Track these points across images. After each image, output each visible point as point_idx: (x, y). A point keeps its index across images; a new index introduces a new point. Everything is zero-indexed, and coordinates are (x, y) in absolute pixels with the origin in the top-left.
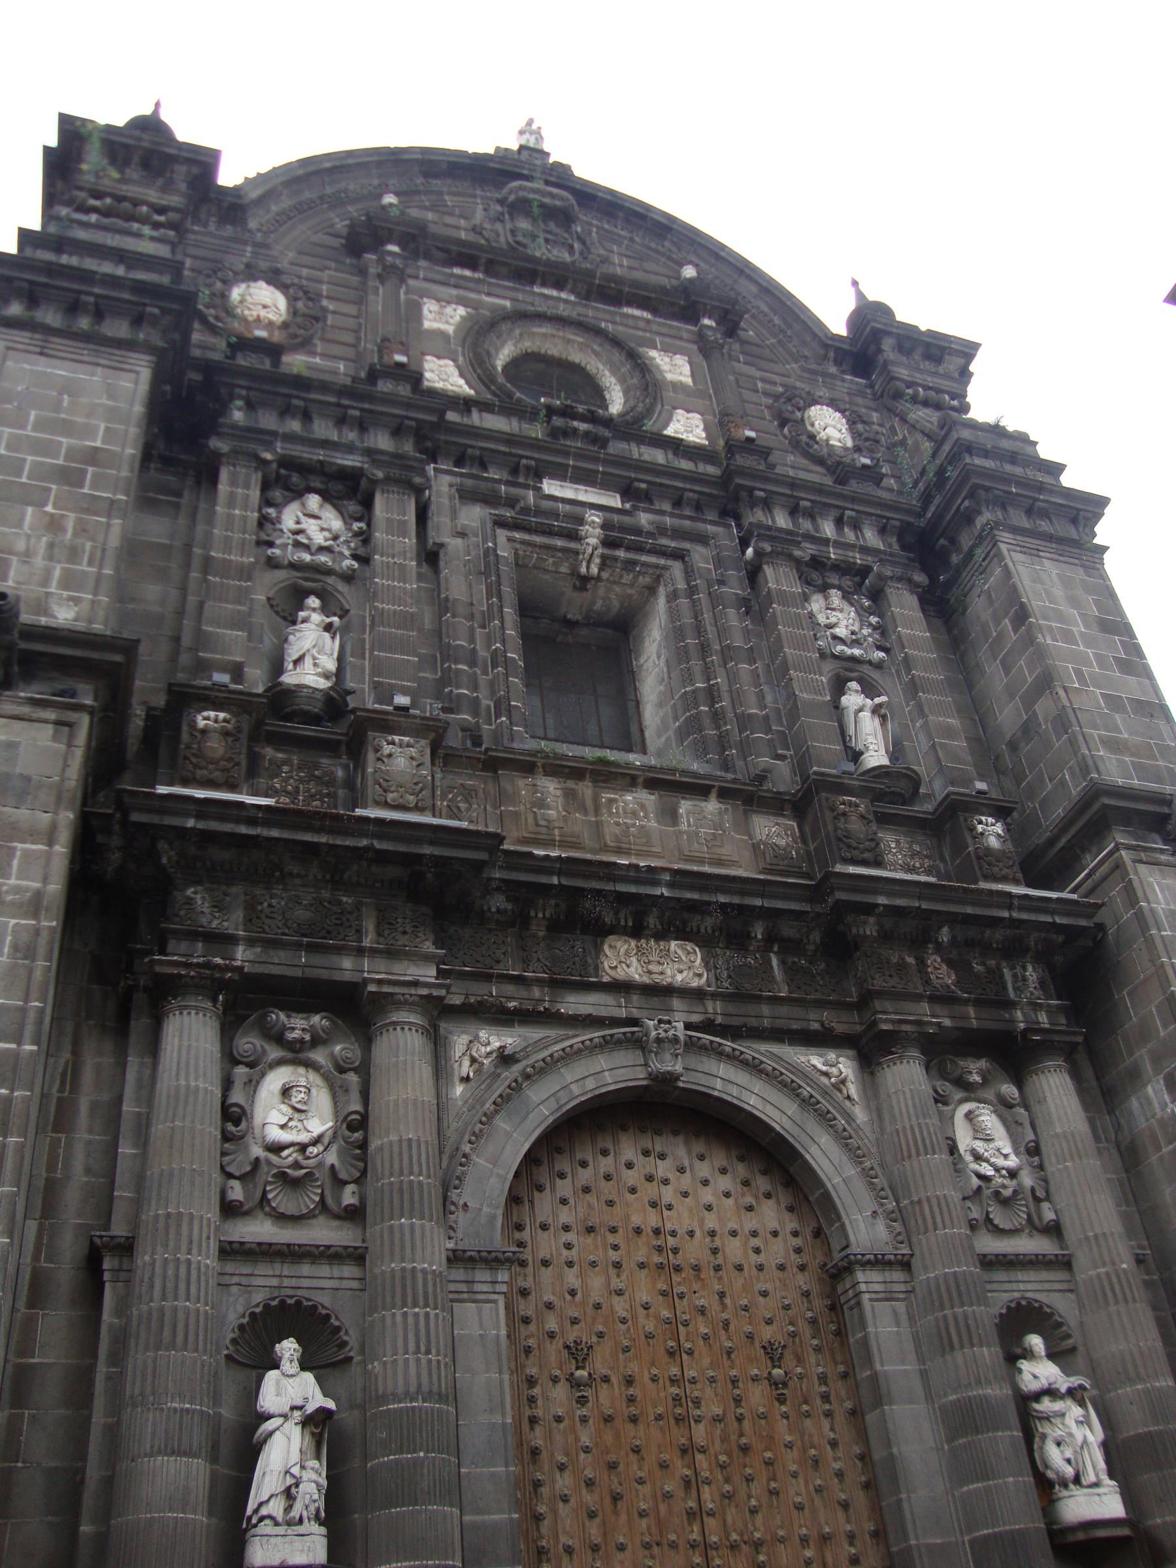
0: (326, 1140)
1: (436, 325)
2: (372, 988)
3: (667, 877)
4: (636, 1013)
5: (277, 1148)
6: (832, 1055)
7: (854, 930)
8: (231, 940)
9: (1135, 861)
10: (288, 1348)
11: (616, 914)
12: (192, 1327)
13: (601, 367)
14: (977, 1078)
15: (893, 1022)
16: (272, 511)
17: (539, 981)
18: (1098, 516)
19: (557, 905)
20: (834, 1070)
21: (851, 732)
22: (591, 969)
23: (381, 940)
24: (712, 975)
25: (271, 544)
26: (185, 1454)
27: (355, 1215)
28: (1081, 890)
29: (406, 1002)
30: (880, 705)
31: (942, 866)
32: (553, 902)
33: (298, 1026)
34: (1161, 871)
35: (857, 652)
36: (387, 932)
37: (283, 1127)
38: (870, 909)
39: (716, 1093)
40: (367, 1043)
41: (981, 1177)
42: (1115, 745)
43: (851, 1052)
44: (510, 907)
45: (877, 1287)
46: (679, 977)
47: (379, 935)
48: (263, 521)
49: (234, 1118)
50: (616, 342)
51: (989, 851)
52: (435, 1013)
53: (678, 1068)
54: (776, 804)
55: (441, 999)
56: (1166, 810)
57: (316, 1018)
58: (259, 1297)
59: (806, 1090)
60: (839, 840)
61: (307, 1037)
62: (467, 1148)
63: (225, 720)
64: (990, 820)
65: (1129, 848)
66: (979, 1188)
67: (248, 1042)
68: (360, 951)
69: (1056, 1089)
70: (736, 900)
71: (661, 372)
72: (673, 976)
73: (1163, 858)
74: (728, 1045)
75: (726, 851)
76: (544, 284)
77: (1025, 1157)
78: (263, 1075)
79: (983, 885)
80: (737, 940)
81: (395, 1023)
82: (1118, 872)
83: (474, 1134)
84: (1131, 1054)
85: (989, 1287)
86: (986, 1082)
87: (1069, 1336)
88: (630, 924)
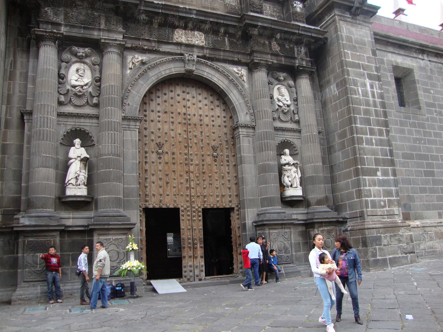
0: (89, 85)
2: (103, 41)
3: (195, 12)
4: (183, 52)
5: (74, 87)
6: (240, 68)
7: (251, 32)
8: (59, 25)
9: (340, 20)
10: (77, 141)
11: (179, 22)
12: (49, 135)
14: (282, 78)
15: (259, 60)
17: (154, 41)
19: (161, 19)
20: (240, 72)
22: (170, 38)
23: (106, 26)
24: (207, 42)
26: (47, 167)
27: (96, 106)
28: (323, 27)
29: (113, 45)
31: (282, 16)
32: (160, 18)
33: (81, 51)
34: (347, 24)
36: (108, 24)
37: (76, 81)
38: (256, 26)
39: (205, 76)
40: (102, 57)
41: (279, 106)
43: (246, 68)
44: (147, 18)
45: (245, 133)
46: (197, 42)
47: (106, 25)
49: (61, 77)
51: (296, 12)
52: (122, 49)
53: (194, 68)
55: (124, 45)
56: (352, 5)
57: (86, 49)
58: (69, 128)
59: (231, 77)
60: (250, 5)
61: (84, 55)
62: (130, 88)
64: (299, 3)
65: (338, 15)
66: (278, 109)
67: (66, 56)
68: (100, 30)
69: (305, 83)
70: (216, 20)
72: (195, 42)
73: (348, 20)
74: (209, 63)
75: (216, 5)
77: (293, 102)
78: (71, 65)
79: (293, 22)
80: (216, 32)
81: (109, 52)
82: (334, 23)
83: (132, 84)
84: (329, 76)
85: (277, 136)
86: (285, 79)
87: (297, 150)
88: (183, 25)
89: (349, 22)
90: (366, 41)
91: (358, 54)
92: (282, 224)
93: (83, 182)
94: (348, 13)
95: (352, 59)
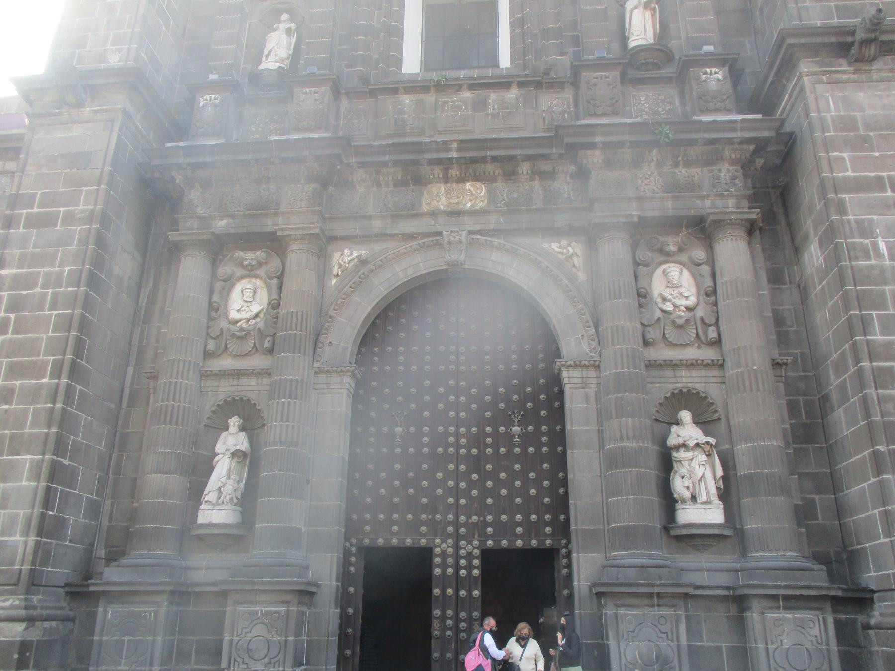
4: (439, 228)
6: (564, 242)
10: (234, 422)
12: (175, 414)
14: (672, 248)
21: (627, 25)
26: (166, 473)
27: (271, 351)
33: (249, 257)
37: (238, 311)
41: (663, 311)
45: (576, 381)
53: (462, 258)
54: (556, 85)
56: (850, 39)
57: (259, 253)
58: (221, 397)
61: (254, 263)
64: (713, 70)
66: (659, 319)
73: (845, 76)
74: (496, 241)
84: (805, 224)
85: (649, 380)
86: (681, 250)
87: (716, 411)
89: (848, 81)
90: (859, 119)
91: (877, 154)
92: (650, 596)
93: (228, 497)
94: (843, 61)
95: (853, 171)
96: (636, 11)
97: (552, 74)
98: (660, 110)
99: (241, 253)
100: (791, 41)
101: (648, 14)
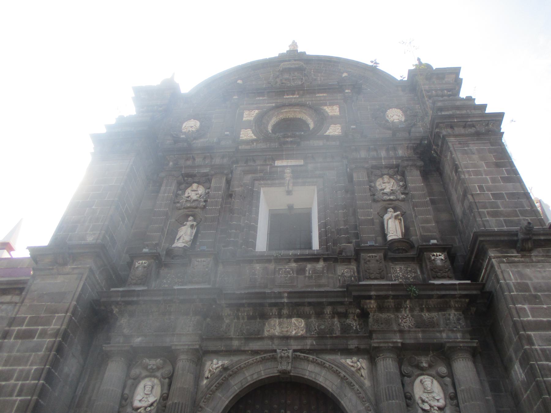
1: (247, 119)
4: (275, 347)
6: (355, 359)
9: (499, 263)
13: (307, 117)
14: (425, 365)
15: (377, 343)
16: (180, 192)
18: (500, 122)
20: (355, 365)
21: (386, 228)
25: (178, 202)
30: (397, 216)
33: (153, 363)
35: (392, 197)
37: (140, 401)
38: (370, 297)
39: (306, 377)
42: (495, 214)
48: (177, 196)
50: (310, 107)
53: (289, 368)
54: (347, 260)
56: (515, 238)
57: (159, 360)
59: (343, 374)
61: (154, 367)
63: (145, 263)
64: (438, 254)
69: (464, 368)
71: (327, 113)
73: (516, 259)
74: (311, 357)
76: (288, 95)
77: (448, 401)
86: (430, 366)
89: (519, 262)
91: (545, 306)
94: (514, 251)
95: (533, 317)
96: (390, 220)
97: (344, 254)
98: (409, 276)
99: (147, 360)
100: (482, 239)
101: (397, 222)
